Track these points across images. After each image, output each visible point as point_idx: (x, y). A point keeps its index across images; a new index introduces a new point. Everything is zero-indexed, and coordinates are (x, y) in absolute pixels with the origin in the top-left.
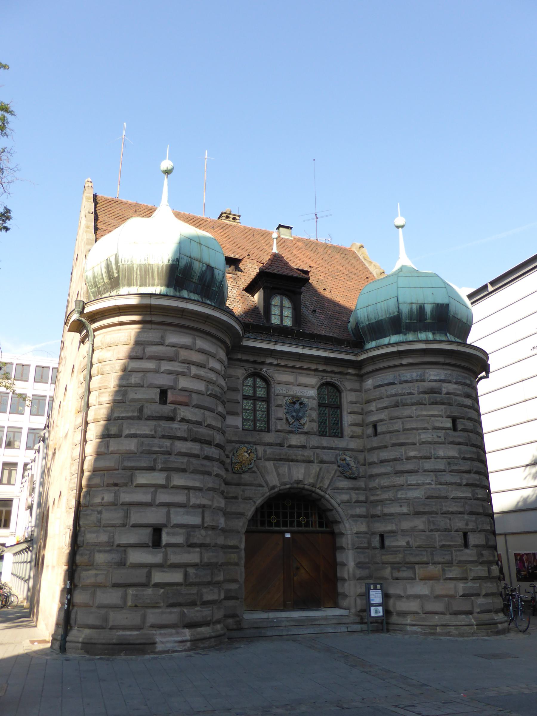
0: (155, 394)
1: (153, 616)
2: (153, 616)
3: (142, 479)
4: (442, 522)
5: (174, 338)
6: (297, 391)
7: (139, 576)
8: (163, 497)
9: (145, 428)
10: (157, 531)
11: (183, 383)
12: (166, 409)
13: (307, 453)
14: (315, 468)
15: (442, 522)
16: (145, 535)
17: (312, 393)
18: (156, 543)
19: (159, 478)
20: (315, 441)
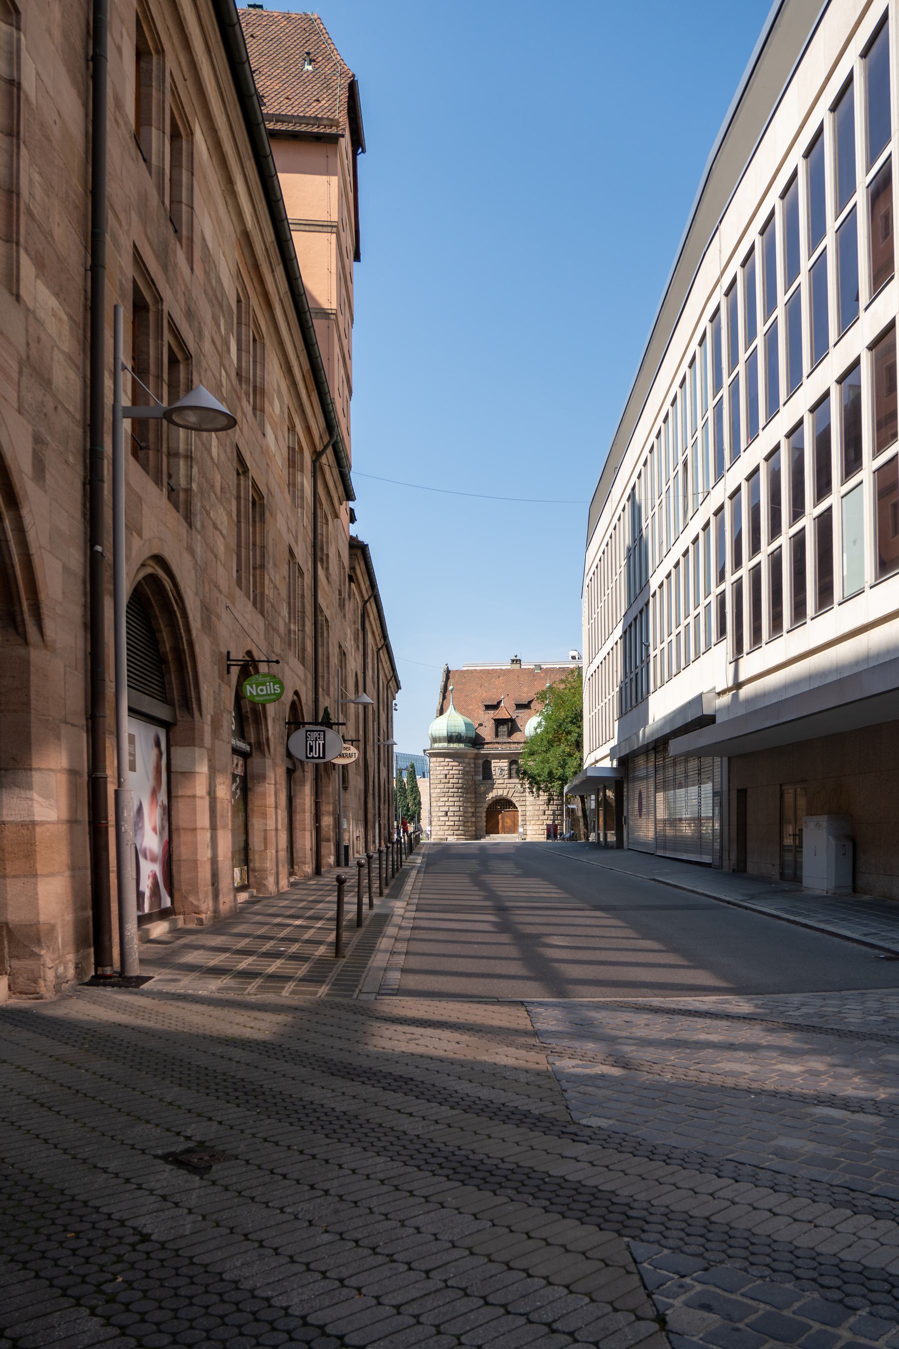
0: (443, 776)
1: (447, 833)
2: (447, 833)
3: (442, 799)
4: (537, 808)
5: (447, 760)
6: (501, 764)
7: (443, 823)
8: (447, 804)
9: (442, 786)
10: (447, 812)
11: (451, 772)
12: (447, 781)
13: (504, 786)
14: (506, 791)
15: (537, 808)
16: (443, 814)
17: (506, 764)
18: (446, 815)
19: (446, 799)
20: (506, 781)
